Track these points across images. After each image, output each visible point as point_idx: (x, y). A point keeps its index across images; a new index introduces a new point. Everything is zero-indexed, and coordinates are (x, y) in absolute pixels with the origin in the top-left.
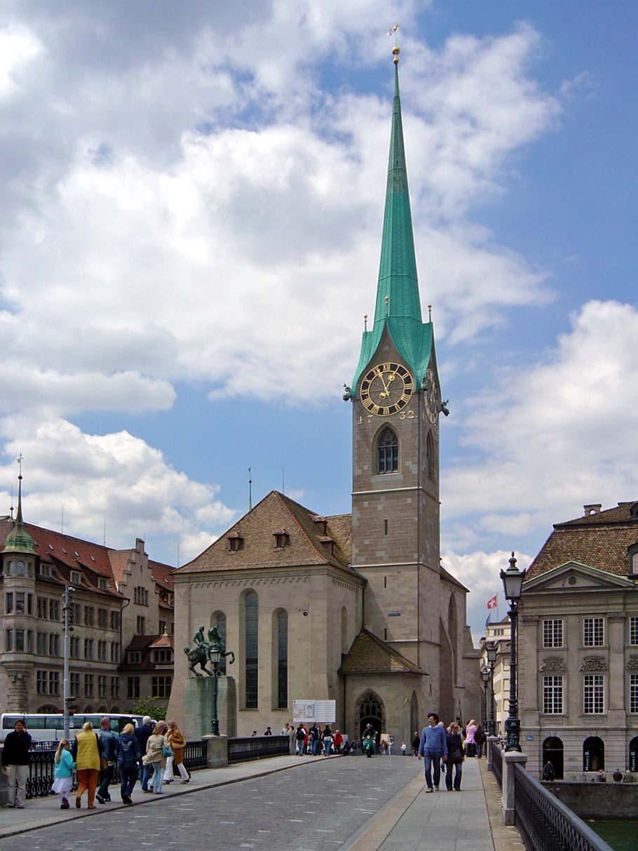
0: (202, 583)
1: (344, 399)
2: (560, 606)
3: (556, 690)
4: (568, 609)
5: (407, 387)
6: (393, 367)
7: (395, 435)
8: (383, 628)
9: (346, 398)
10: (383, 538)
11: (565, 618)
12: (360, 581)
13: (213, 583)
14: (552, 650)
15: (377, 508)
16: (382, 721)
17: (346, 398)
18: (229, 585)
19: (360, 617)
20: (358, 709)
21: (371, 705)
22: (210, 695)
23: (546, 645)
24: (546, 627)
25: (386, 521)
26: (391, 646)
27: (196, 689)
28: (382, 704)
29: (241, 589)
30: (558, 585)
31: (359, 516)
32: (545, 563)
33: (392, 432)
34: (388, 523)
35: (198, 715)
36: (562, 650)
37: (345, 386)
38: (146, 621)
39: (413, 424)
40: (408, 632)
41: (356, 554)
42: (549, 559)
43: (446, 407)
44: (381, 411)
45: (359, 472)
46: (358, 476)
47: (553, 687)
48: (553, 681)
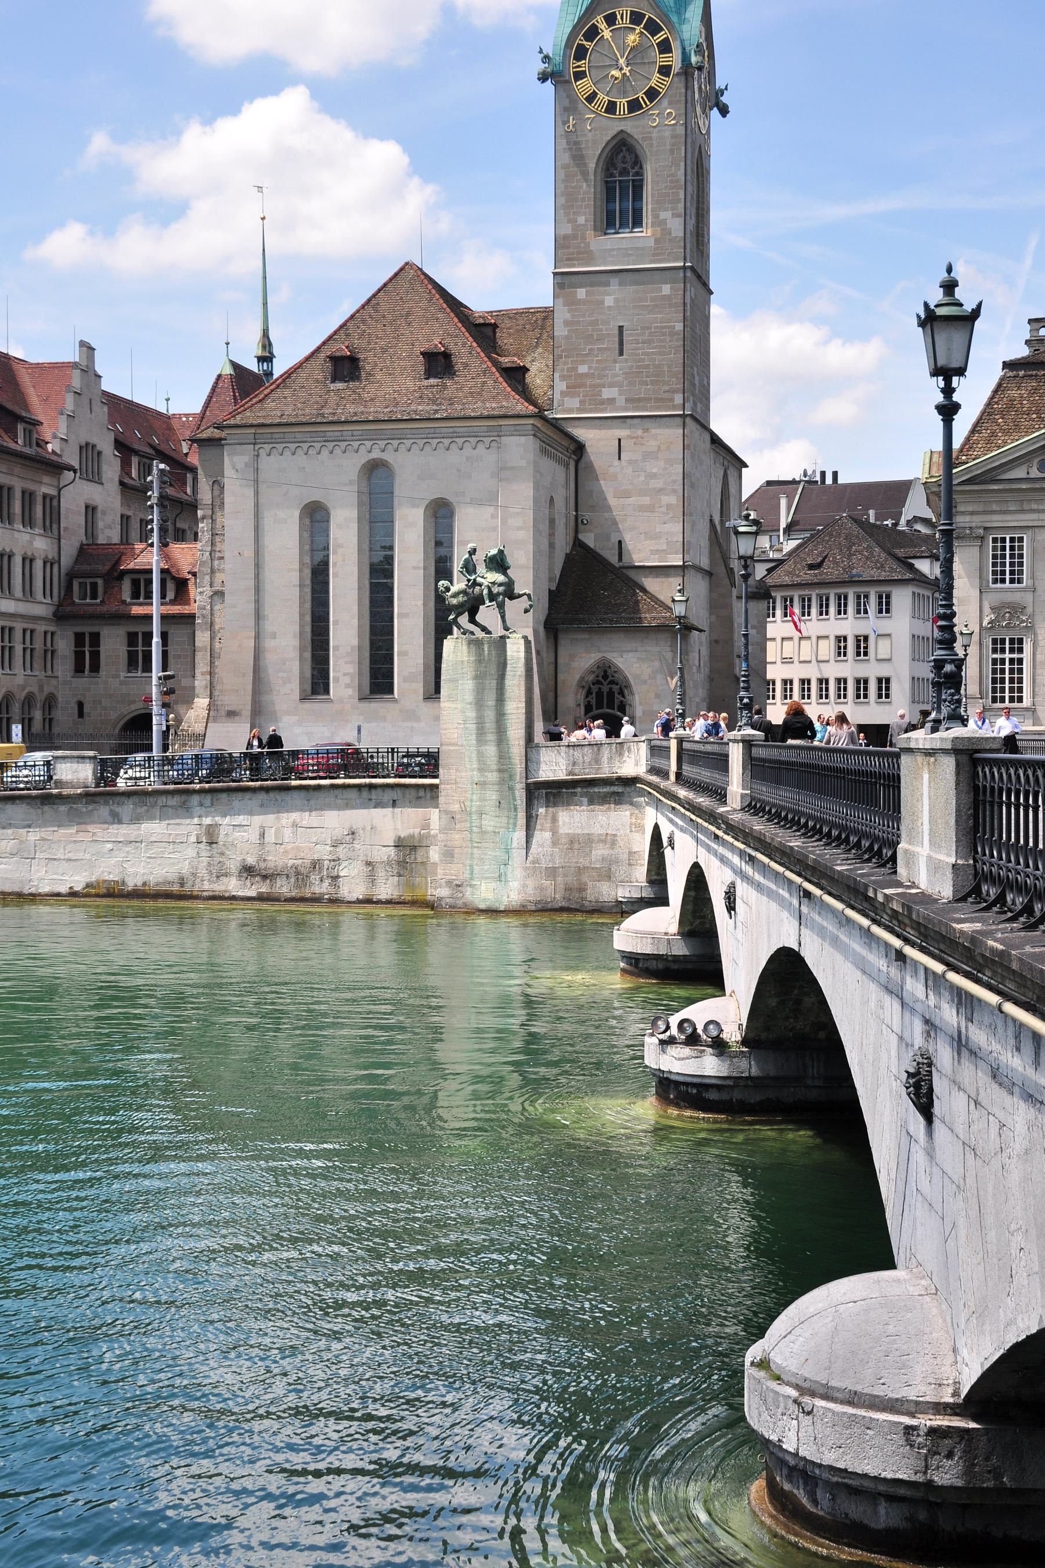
0: (280, 447)
1: (539, 79)
2: (1022, 511)
3: (1012, 661)
4: (1034, 516)
5: (662, 60)
6: (636, 18)
7: (637, 157)
8: (614, 540)
9: (543, 78)
10: (615, 361)
11: (1030, 532)
12: (572, 447)
13: (305, 446)
14: (1006, 590)
15: (603, 302)
17: (543, 78)
20: (581, 696)
22: (493, 669)
24: (994, 549)
26: (632, 574)
27: (466, 659)
29: (363, 457)
30: (1019, 473)
31: (568, 316)
35: (471, 703)
36: (1024, 590)
37: (541, 51)
39: (674, 137)
40: (664, 547)
41: (562, 392)
43: (724, 99)
44: (611, 108)
45: (567, 229)
46: (566, 237)
47: (1007, 656)
48: (1007, 646)
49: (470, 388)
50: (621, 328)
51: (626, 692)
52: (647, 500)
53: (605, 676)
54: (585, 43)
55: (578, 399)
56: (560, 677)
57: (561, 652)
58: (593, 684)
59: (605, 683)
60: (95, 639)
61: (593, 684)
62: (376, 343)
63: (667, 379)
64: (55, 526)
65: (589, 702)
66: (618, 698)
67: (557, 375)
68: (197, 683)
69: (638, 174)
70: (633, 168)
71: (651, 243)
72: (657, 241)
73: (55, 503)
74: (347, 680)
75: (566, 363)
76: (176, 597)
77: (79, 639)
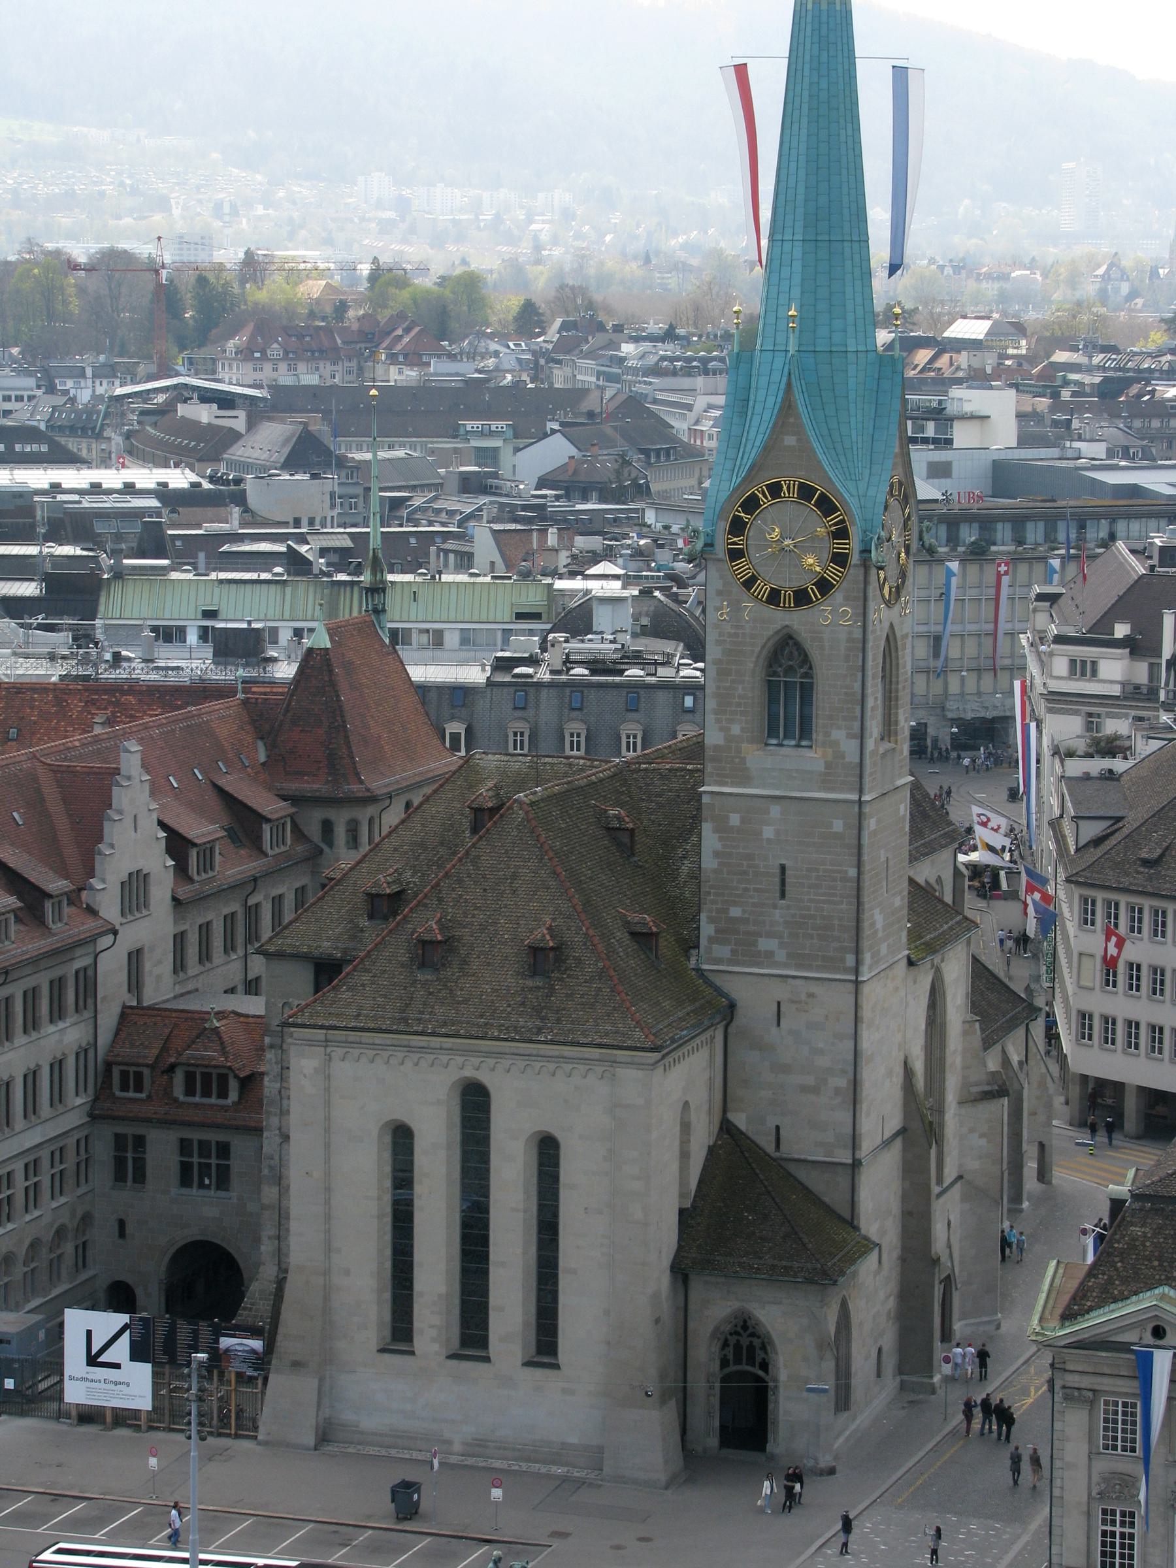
3: (1123, 1535)
7: (806, 655)
8: (771, 1122)
10: (775, 907)
16: (771, 1384)
18: (423, 1063)
19: (718, 1096)
20: (716, 1347)
21: (745, 1341)
23: (1106, 1447)
24: (1106, 1412)
25: (783, 868)
26: (792, 1168)
28: (771, 1342)
31: (718, 846)
32: (1110, 1278)
33: (797, 645)
34: (788, 872)
38: (146, 955)
39: (850, 640)
42: (1116, 1269)
46: (717, 748)
47: (1118, 1529)
49: (582, 996)
50: (783, 868)
51: (769, 1348)
52: (810, 1080)
53: (745, 1327)
54: (742, 515)
55: (730, 947)
56: (691, 1325)
57: (693, 1295)
58: (731, 1334)
59: (745, 1335)
60: (140, 1141)
61: (731, 1334)
62: (474, 916)
63: (836, 933)
64: (90, 1001)
65: (725, 1355)
66: (760, 1355)
67: (703, 917)
68: (263, 1248)
69: (806, 675)
70: (801, 667)
71: (820, 767)
72: (828, 766)
73: (90, 972)
74: (433, 1333)
75: (713, 902)
76: (240, 1098)
77: (120, 1141)
